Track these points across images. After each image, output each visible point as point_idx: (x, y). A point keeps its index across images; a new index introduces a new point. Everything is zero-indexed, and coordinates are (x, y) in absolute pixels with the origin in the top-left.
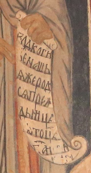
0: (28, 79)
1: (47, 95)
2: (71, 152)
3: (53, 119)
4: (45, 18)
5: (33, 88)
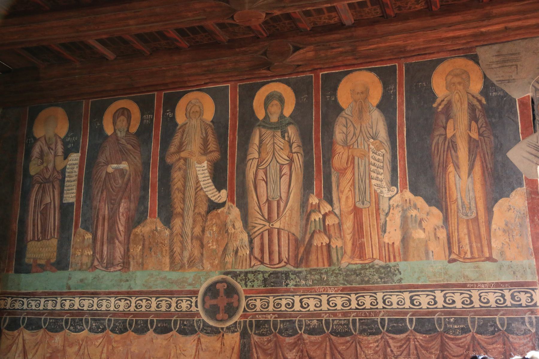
0: (374, 165)
1: (381, 171)
2: (390, 193)
3: (384, 180)
4: (380, 141)
5: (376, 168)
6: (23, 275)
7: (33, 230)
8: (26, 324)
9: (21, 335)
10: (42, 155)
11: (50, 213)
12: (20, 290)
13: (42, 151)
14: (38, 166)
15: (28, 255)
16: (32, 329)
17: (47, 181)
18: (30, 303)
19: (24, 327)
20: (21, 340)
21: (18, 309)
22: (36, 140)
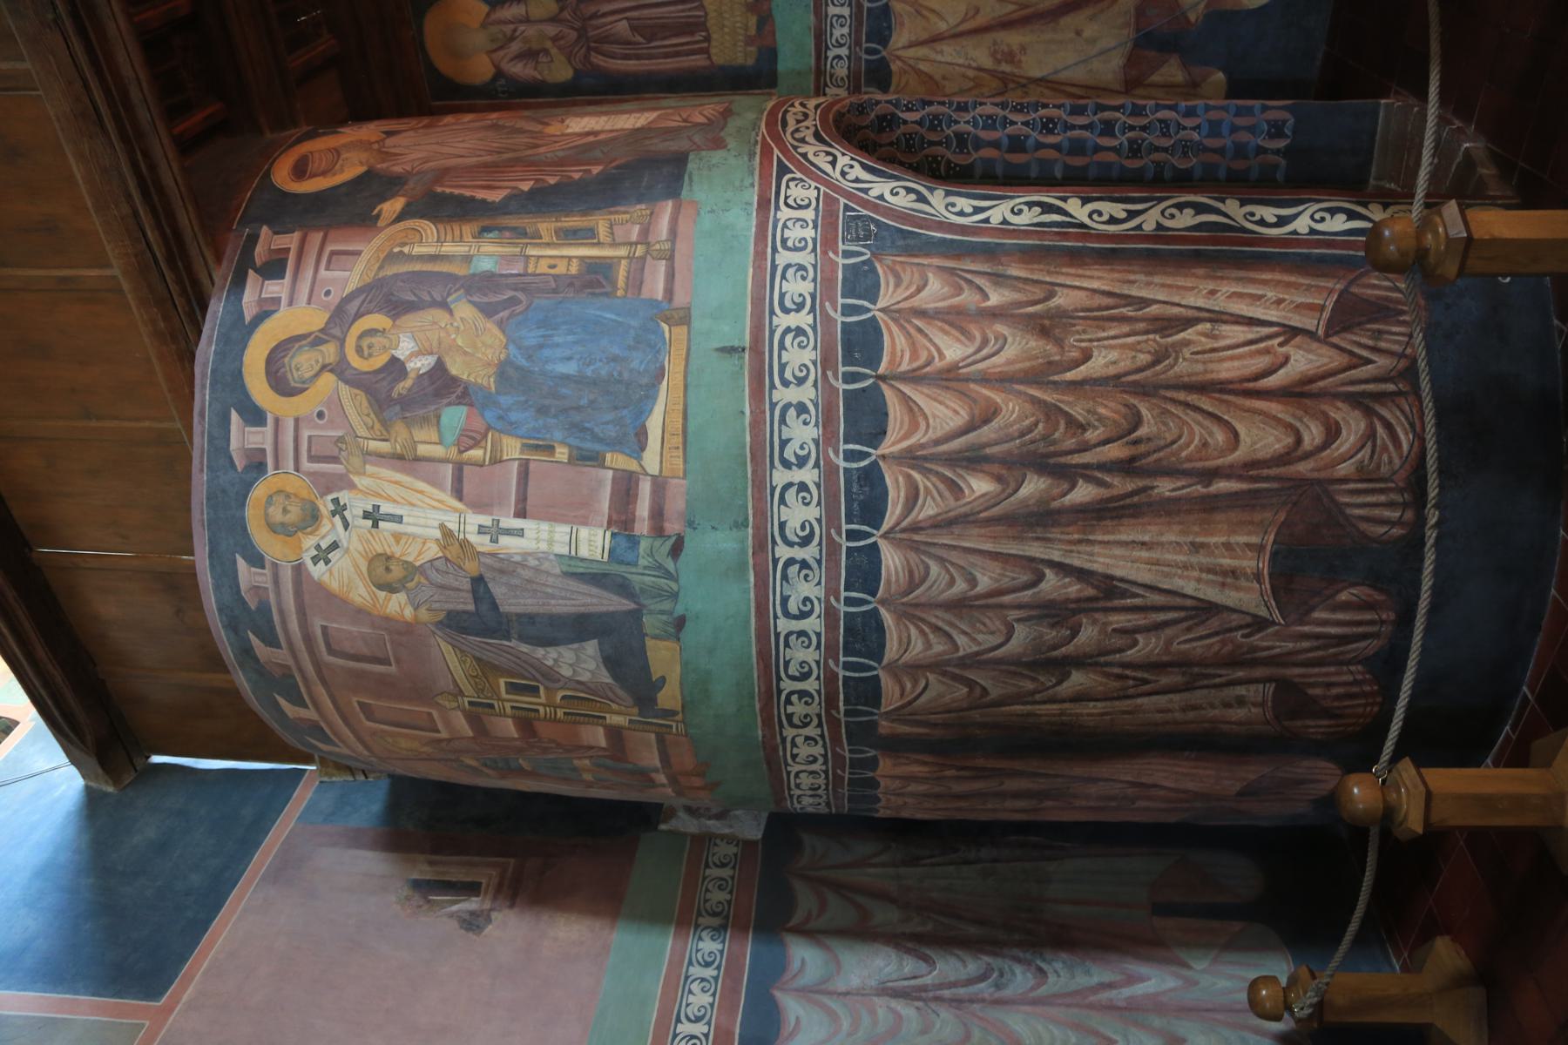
6: (781, 67)
7: (687, 55)
8: (879, 44)
9: (899, 53)
10: (529, 55)
11: (650, 19)
12: (811, 69)
13: (520, 57)
14: (552, 61)
15: (740, 60)
16: (890, 28)
17: (582, 32)
18: (837, 41)
19: (885, 47)
20: (911, 52)
21: (849, 68)
22: (499, 74)
